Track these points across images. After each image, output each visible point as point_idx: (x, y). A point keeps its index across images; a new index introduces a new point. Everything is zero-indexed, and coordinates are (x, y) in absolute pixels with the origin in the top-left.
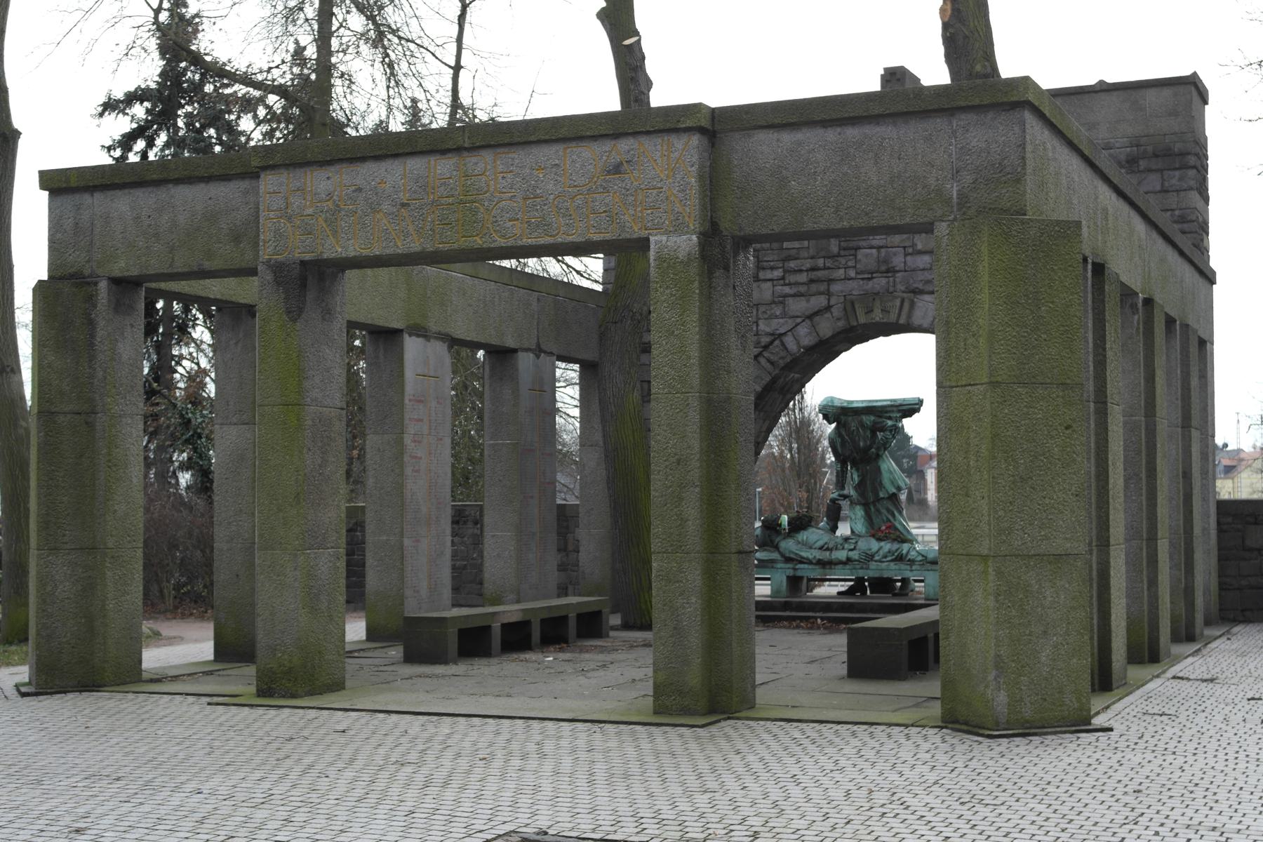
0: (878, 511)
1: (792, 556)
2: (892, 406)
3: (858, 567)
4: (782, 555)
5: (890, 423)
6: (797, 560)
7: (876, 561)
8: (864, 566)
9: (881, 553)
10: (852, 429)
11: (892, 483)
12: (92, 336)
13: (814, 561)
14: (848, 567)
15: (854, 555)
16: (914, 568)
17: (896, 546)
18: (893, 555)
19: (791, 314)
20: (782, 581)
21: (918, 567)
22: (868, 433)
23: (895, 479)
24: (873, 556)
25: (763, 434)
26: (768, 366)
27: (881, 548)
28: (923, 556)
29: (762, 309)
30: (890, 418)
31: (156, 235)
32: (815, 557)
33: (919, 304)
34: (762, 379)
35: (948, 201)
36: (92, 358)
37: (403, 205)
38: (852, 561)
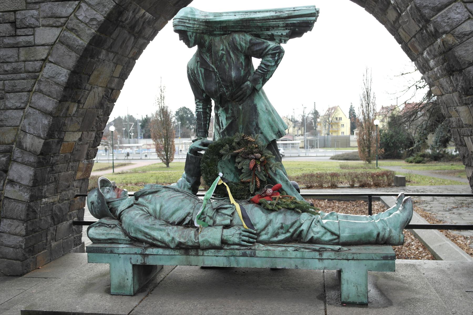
1: (140, 236)
2: (278, 18)
3: (238, 253)
4: (126, 234)
5: (272, 44)
6: (147, 242)
7: (265, 243)
8: (248, 252)
9: (270, 229)
10: (221, 52)
11: (272, 127)
13: (172, 246)
14: (222, 252)
16: (325, 255)
17: (290, 218)
18: (288, 231)
20: (126, 272)
21: (332, 255)
22: (242, 59)
23: (274, 121)
24: (258, 234)
25: (116, 80)
27: (270, 222)
28: (333, 233)
30: (272, 38)
32: (173, 239)
34: (105, 6)
38: (229, 245)
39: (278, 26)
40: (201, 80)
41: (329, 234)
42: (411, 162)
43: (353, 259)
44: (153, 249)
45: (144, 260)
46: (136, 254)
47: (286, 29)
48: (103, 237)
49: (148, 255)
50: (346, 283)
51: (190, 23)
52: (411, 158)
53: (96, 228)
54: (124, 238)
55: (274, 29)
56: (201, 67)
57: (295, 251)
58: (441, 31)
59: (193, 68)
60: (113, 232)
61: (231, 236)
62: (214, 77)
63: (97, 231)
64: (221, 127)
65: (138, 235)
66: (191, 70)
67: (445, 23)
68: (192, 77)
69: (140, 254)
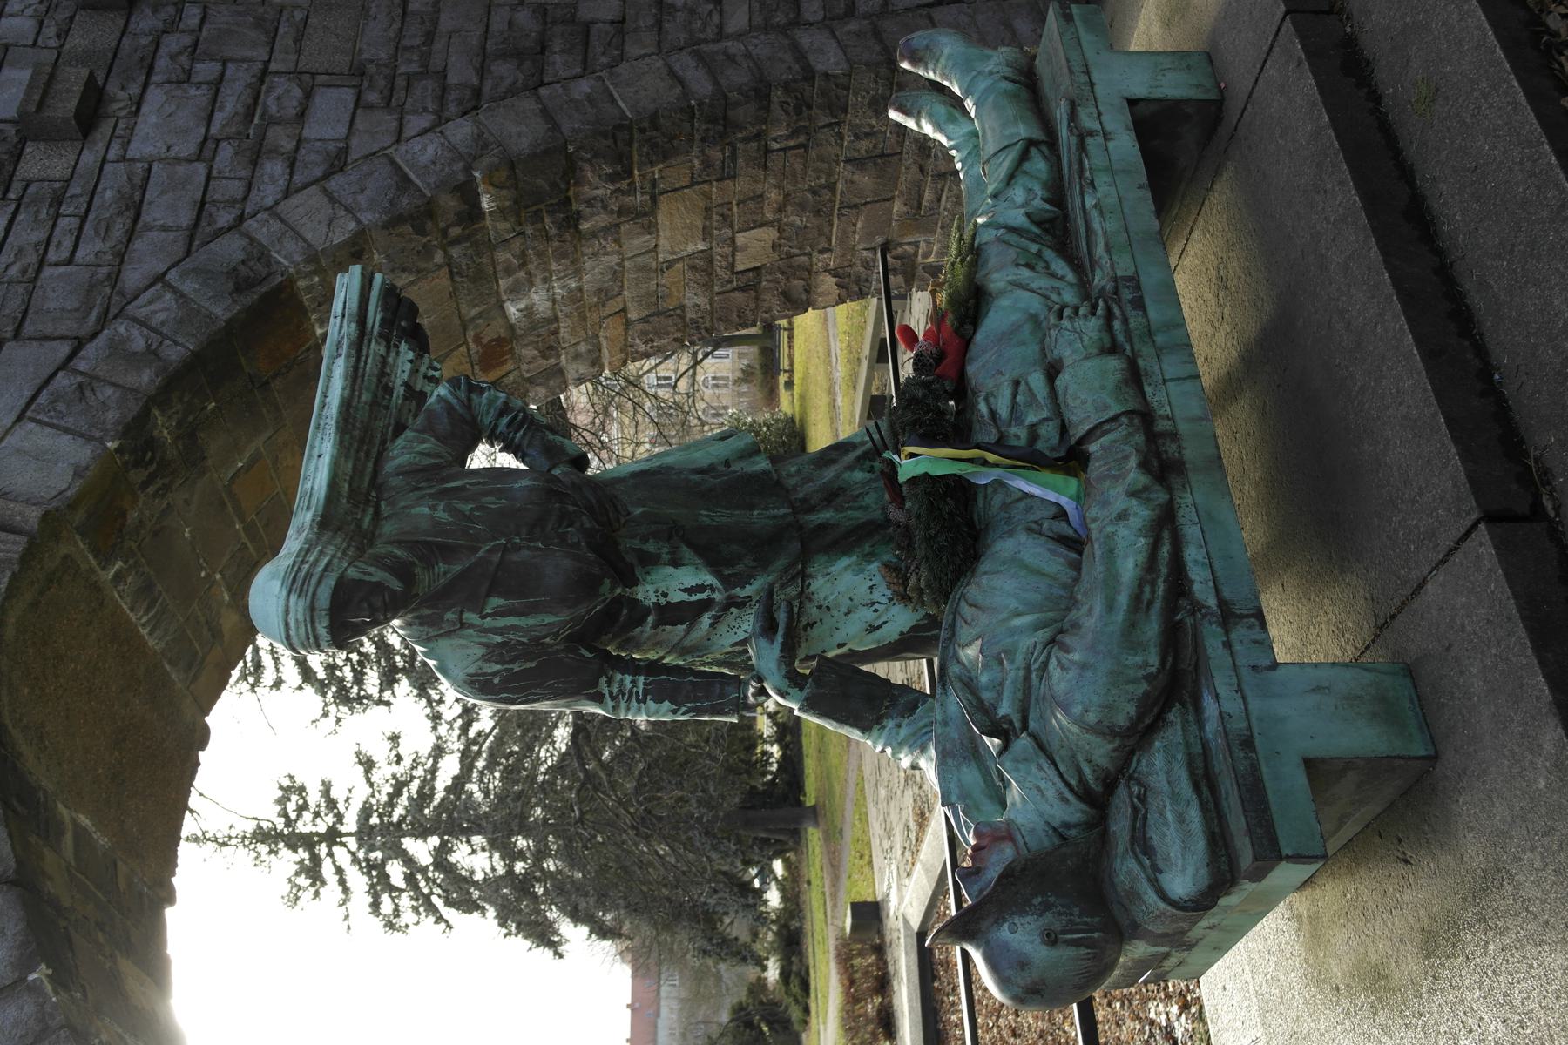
1: (1152, 628)
3: (1135, 321)
6: (1171, 608)
8: (1127, 295)
13: (1161, 496)
28: (1024, 156)
32: (1133, 494)
39: (384, 361)
40: (530, 621)
41: (1027, 166)
42: (807, 1010)
43: (1088, 73)
44: (1191, 582)
45: (1247, 616)
46: (1228, 645)
47: (397, 347)
48: (1194, 814)
49: (1222, 603)
50: (1160, 90)
51: (316, 561)
52: (795, 1014)
53: (1160, 864)
54: (1179, 728)
55: (389, 375)
56: (483, 609)
57: (1094, 187)
58: (461, 177)
59: (480, 651)
60: (1162, 778)
61: (1085, 338)
62: (525, 553)
63: (1175, 852)
64: (704, 596)
65: (1150, 634)
66: (489, 661)
67: (443, 169)
68: (512, 661)
69: (1227, 633)
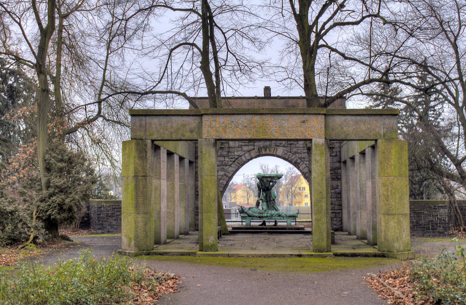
0: (270, 203)
5: (274, 180)
12: (146, 155)
15: (268, 215)
19: (244, 150)
26: (237, 164)
29: (236, 149)
31: (167, 129)
33: (278, 149)
35: (381, 135)
36: (146, 161)
37: (245, 127)
